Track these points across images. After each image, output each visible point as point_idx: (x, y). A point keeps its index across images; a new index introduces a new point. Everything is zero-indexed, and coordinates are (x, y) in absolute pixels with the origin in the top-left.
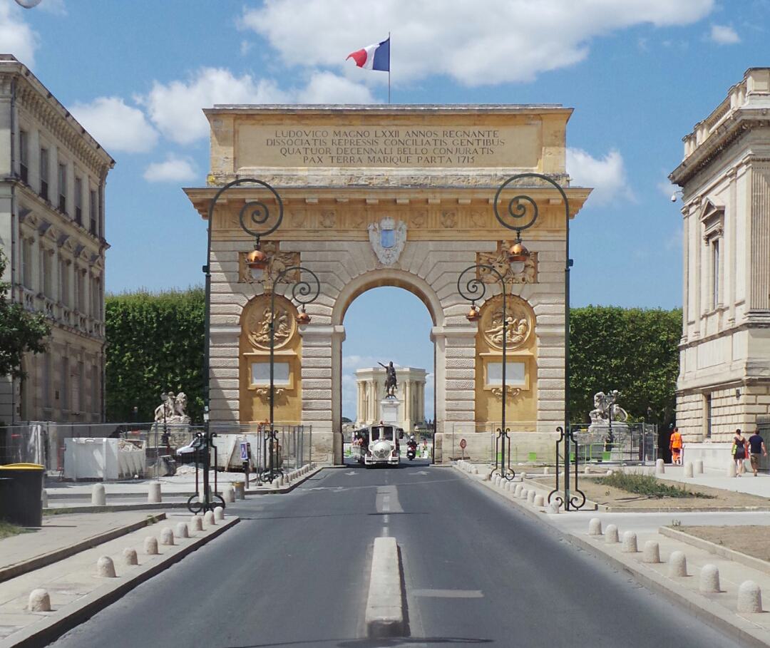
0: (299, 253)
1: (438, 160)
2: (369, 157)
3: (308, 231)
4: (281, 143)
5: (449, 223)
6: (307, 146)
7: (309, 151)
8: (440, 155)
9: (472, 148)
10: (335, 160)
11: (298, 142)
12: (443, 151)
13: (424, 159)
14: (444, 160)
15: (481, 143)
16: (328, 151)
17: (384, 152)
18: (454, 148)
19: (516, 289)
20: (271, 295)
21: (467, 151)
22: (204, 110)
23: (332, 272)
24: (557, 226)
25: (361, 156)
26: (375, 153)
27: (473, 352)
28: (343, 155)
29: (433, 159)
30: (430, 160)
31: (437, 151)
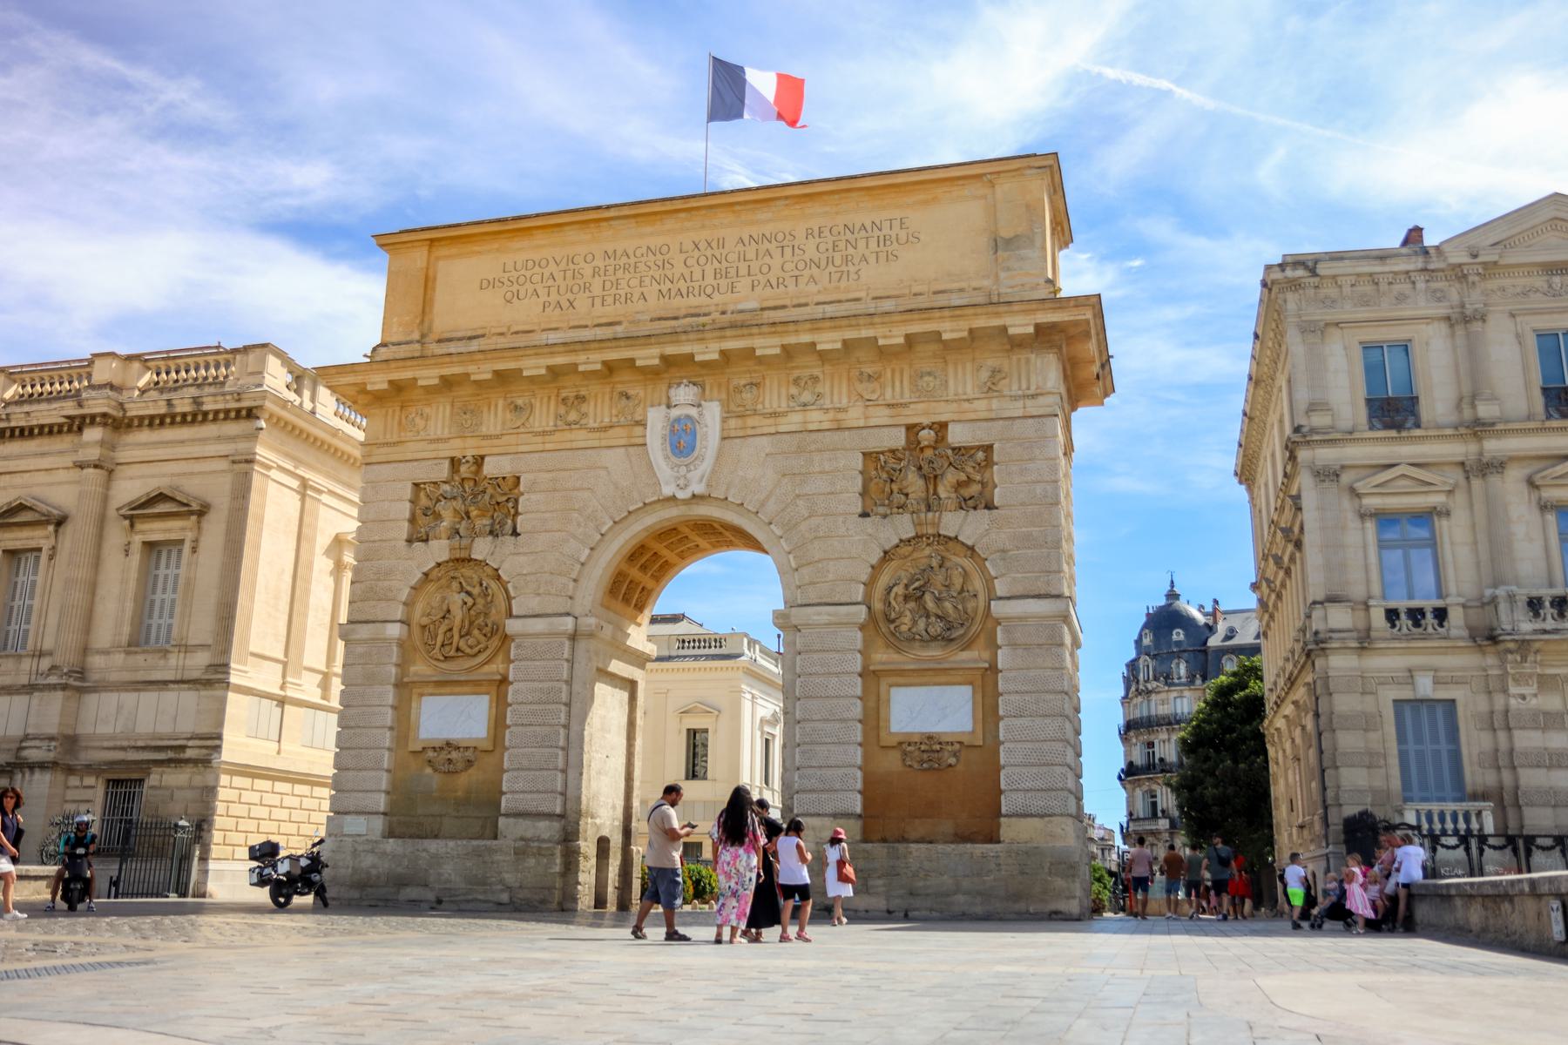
0: (518, 478)
1: (790, 283)
3: (537, 434)
5: (807, 397)
6: (550, 282)
8: (797, 273)
10: (598, 301)
11: (537, 278)
12: (801, 265)
17: (688, 280)
19: (952, 522)
21: (846, 260)
24: (1033, 387)
27: (857, 663)
28: (613, 291)
30: (774, 284)
31: (789, 266)
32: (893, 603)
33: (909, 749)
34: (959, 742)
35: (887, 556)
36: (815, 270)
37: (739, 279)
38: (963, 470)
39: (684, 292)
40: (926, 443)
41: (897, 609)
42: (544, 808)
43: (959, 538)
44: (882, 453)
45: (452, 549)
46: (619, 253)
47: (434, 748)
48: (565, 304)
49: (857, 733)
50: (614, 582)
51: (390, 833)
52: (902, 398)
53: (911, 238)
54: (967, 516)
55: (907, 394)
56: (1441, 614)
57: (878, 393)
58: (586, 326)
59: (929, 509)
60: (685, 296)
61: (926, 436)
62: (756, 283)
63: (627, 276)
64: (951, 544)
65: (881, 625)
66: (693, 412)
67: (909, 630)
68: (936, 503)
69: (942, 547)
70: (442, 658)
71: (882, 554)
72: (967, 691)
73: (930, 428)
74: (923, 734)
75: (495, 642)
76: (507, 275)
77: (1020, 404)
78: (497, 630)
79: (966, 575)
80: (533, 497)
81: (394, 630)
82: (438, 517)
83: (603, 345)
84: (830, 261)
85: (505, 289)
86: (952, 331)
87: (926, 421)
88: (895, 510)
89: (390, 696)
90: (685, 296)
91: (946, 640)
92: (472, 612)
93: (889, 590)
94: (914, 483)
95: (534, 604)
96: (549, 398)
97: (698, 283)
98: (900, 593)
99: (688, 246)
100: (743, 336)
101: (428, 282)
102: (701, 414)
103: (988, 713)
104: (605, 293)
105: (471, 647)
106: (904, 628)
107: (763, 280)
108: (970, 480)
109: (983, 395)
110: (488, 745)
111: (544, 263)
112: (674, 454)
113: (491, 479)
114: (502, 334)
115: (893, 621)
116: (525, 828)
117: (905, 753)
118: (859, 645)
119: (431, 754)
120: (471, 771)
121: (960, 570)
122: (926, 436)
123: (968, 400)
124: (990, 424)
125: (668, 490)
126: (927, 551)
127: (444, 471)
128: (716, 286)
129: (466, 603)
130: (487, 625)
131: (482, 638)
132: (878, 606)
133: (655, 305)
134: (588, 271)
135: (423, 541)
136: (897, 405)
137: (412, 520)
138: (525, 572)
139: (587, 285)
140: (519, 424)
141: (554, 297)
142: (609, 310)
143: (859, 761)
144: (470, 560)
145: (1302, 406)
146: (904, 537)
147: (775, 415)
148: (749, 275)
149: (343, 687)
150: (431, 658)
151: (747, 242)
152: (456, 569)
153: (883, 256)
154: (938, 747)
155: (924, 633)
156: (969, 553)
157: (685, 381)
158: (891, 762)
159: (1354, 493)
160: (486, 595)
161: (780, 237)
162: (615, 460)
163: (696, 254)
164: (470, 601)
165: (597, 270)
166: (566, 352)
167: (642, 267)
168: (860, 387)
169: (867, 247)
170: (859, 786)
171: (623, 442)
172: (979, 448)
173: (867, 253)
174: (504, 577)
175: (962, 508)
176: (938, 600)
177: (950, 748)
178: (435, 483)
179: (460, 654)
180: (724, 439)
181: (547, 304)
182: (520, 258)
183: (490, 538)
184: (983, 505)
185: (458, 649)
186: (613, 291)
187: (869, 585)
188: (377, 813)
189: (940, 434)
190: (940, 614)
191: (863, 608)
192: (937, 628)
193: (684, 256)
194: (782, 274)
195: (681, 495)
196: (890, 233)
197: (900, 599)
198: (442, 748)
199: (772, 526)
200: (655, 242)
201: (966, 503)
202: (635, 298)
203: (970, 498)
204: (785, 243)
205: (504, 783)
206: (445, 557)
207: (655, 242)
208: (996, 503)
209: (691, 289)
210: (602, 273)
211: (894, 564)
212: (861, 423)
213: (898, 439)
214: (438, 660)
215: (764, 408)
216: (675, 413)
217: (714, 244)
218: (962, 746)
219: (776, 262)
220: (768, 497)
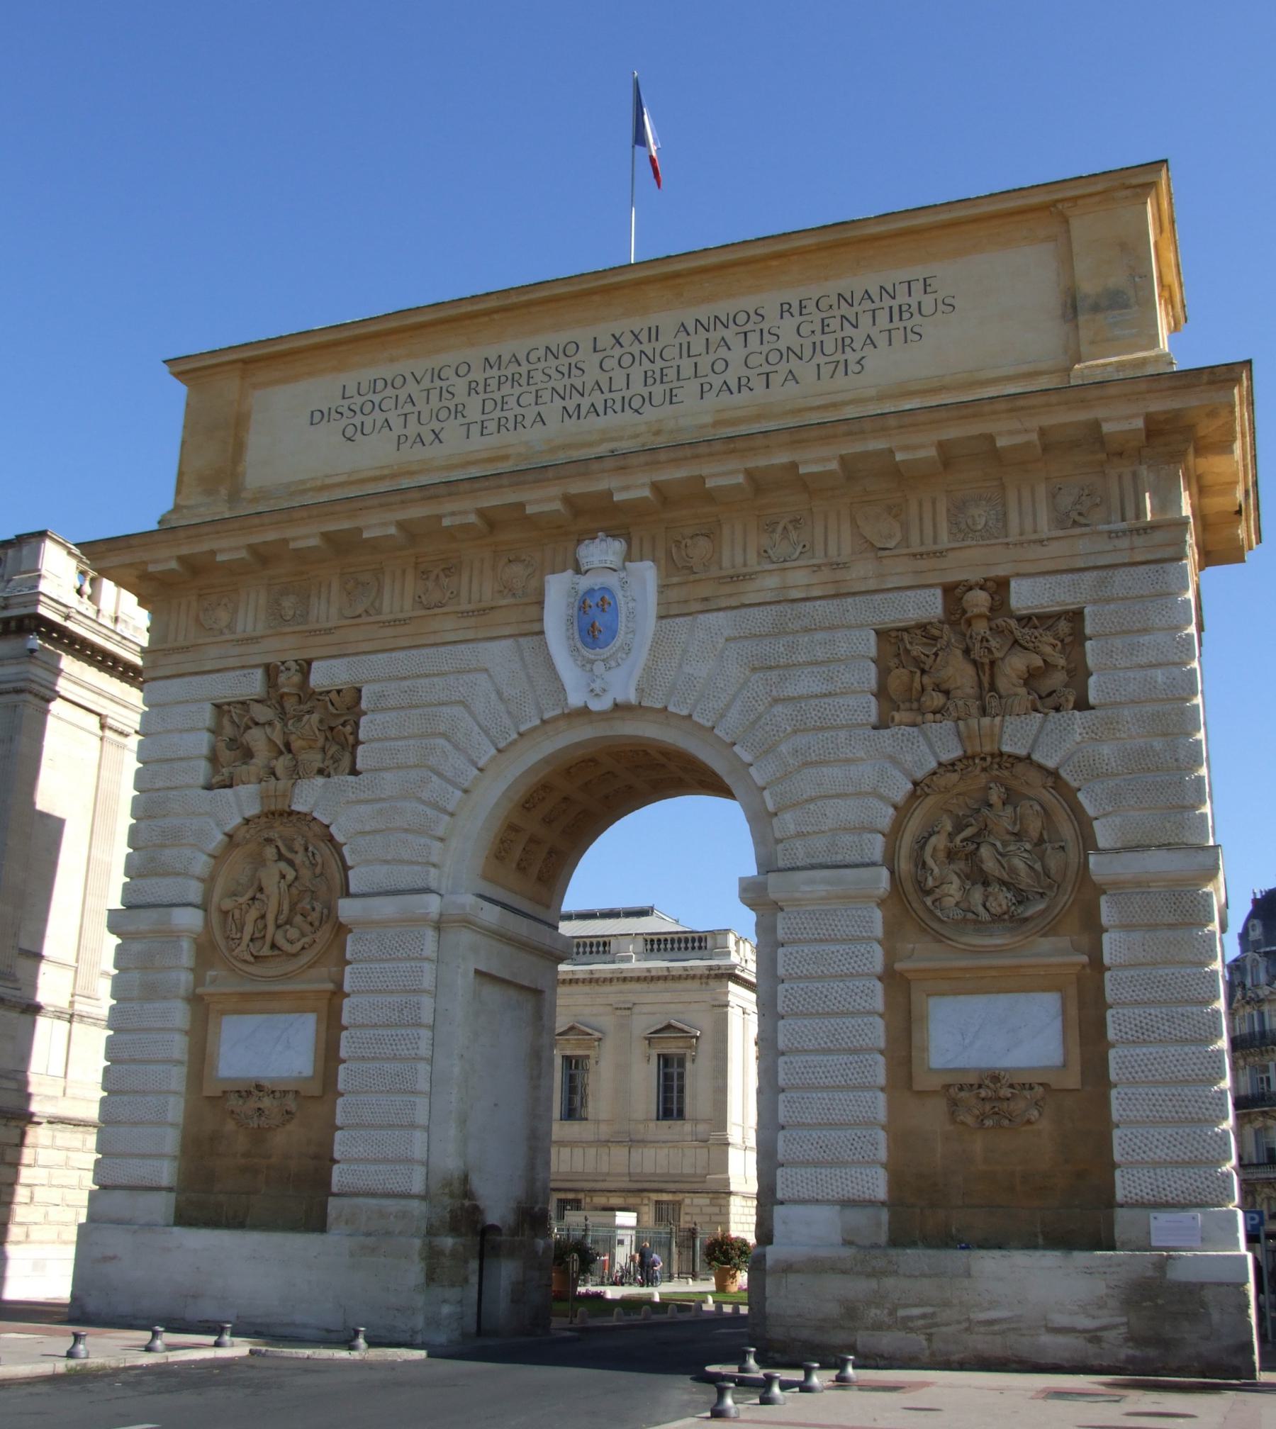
0: (359, 690)
1: (758, 384)
2: (564, 408)
4: (344, 410)
7: (412, 419)
8: (767, 368)
9: (859, 336)
10: (475, 429)
12: (774, 358)
13: (716, 388)
14: (776, 380)
15: (883, 317)
16: (458, 411)
17: (606, 389)
18: (808, 344)
21: (843, 344)
22: (164, 362)
23: (443, 735)
25: (541, 408)
26: (582, 395)
28: (498, 413)
29: (744, 381)
30: (734, 388)
31: (753, 361)
32: (930, 862)
33: (962, 1094)
34: (1041, 1084)
35: (919, 789)
36: (794, 363)
37: (681, 383)
38: (1036, 651)
39: (601, 410)
40: (976, 611)
41: (936, 870)
43: (1035, 757)
44: (906, 630)
45: (264, 797)
46: (505, 359)
47: (238, 1092)
48: (428, 437)
50: (502, 842)
52: (935, 542)
53: (941, 307)
54: (1045, 721)
55: (944, 536)
57: (898, 536)
59: (984, 712)
60: (601, 410)
61: (979, 600)
62: (706, 387)
63: (517, 391)
64: (1020, 768)
66: (612, 580)
67: (957, 904)
68: (995, 703)
69: (1006, 773)
70: (252, 959)
71: (910, 786)
73: (982, 588)
74: (980, 1071)
76: (346, 403)
77: (1124, 543)
78: (328, 916)
79: (1046, 813)
80: (379, 717)
82: (248, 754)
83: (477, 485)
84: (817, 348)
85: (344, 422)
86: (1011, 433)
87: (974, 576)
88: (930, 716)
89: (179, 1014)
90: (601, 410)
92: (294, 891)
93: (922, 842)
94: (959, 673)
95: (378, 875)
96: (404, 572)
97: (620, 394)
98: (941, 846)
99: (605, 341)
100: (686, 459)
102: (624, 583)
104: (485, 417)
105: (292, 942)
106: (949, 902)
107: (717, 381)
109: (1061, 533)
110: (315, 1089)
111: (399, 382)
112: (585, 644)
113: (321, 694)
115: (928, 893)
117: (954, 1104)
118: (879, 931)
119: (234, 1102)
120: (289, 1127)
121: (1037, 807)
122: (979, 600)
123: (1041, 542)
124: (1076, 576)
125: (575, 699)
126: (983, 779)
127: (254, 684)
128: (647, 396)
129: (283, 877)
130: (314, 909)
131: (308, 928)
132: (904, 866)
134: (460, 386)
135: (225, 787)
136: (928, 554)
137: (213, 759)
138: (368, 828)
139: (460, 408)
140: (360, 610)
141: (413, 429)
143: (882, 1115)
144: (291, 813)
146: (946, 757)
147: (734, 578)
148: (696, 377)
149: (114, 1002)
150: (235, 958)
151: (691, 329)
152: (272, 827)
153: (898, 336)
154: (1006, 1092)
155: (981, 909)
156: (1050, 781)
157: (600, 534)
160: (314, 865)
161: (742, 318)
162: (498, 654)
163: (617, 351)
164: (291, 875)
165: (474, 385)
166: (423, 499)
167: (538, 376)
169: (874, 324)
170: (882, 1154)
171: (507, 631)
172: (1058, 616)
173: (874, 333)
174: (340, 838)
175: (1036, 710)
177: (1027, 1093)
178: (243, 703)
179: (276, 952)
180: (661, 617)
181: (402, 439)
182: (367, 375)
183: (320, 780)
184: (1071, 705)
185: (274, 946)
186: (498, 413)
187: (893, 836)
188: (158, 1189)
189: (997, 598)
190: (1006, 877)
191: (885, 873)
192: (1002, 900)
193: (601, 355)
194: (744, 372)
195: (595, 706)
196: (906, 300)
197: (941, 855)
198: (249, 1093)
199: (737, 749)
200: (557, 339)
201: (1048, 702)
202: (527, 423)
203: (1050, 694)
204: (749, 327)
205: (336, 1147)
206: (253, 810)
207: (557, 339)
208: (1092, 699)
209: (610, 403)
210: (481, 388)
211: (930, 801)
212: (872, 585)
213: (929, 606)
214: (245, 961)
215: (721, 569)
216: (585, 583)
217: (644, 337)
219: (737, 353)
220: (728, 706)
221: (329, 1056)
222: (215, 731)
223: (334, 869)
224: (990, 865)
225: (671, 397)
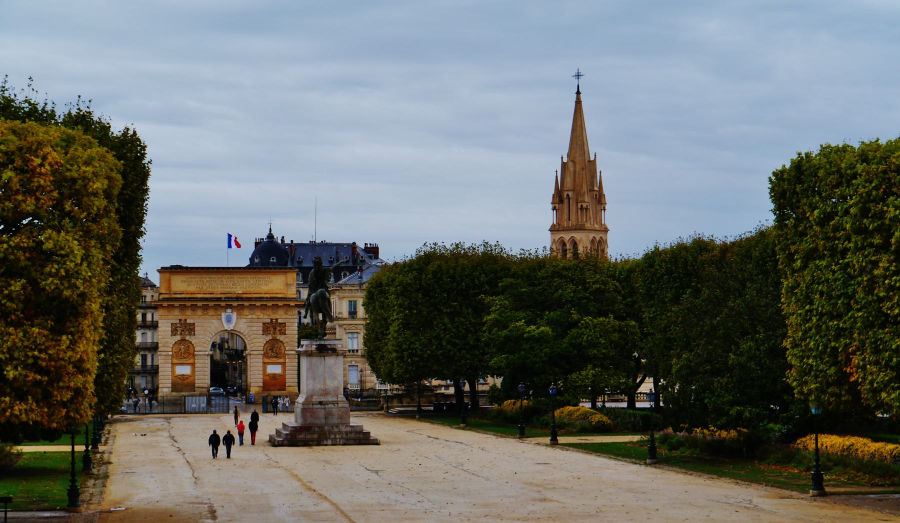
5: (252, 312)
16: (205, 285)
19: (279, 337)
20: (183, 340)
21: (259, 284)
27: (262, 361)
35: (267, 342)
42: (204, 386)
49: (262, 373)
51: (172, 391)
56: (357, 351)
58: (206, 294)
65: (265, 355)
72: (280, 366)
75: (191, 356)
79: (280, 346)
81: (171, 353)
89: (170, 365)
91: (276, 357)
101: (170, 280)
103: (284, 370)
108: (282, 329)
114: (188, 293)
116: (201, 390)
133: (220, 290)
134: (205, 281)
137: (171, 331)
142: (211, 290)
145: (337, 313)
158: (267, 378)
159: (345, 329)
162: (214, 321)
168: (263, 311)
176: (276, 350)
187: (264, 347)
192: (275, 355)
206: (179, 339)
213: (269, 321)
216: (227, 314)
218: (280, 375)
221: (193, 371)
222: (172, 327)
223: (192, 347)
224: (274, 351)
225: (236, 288)
